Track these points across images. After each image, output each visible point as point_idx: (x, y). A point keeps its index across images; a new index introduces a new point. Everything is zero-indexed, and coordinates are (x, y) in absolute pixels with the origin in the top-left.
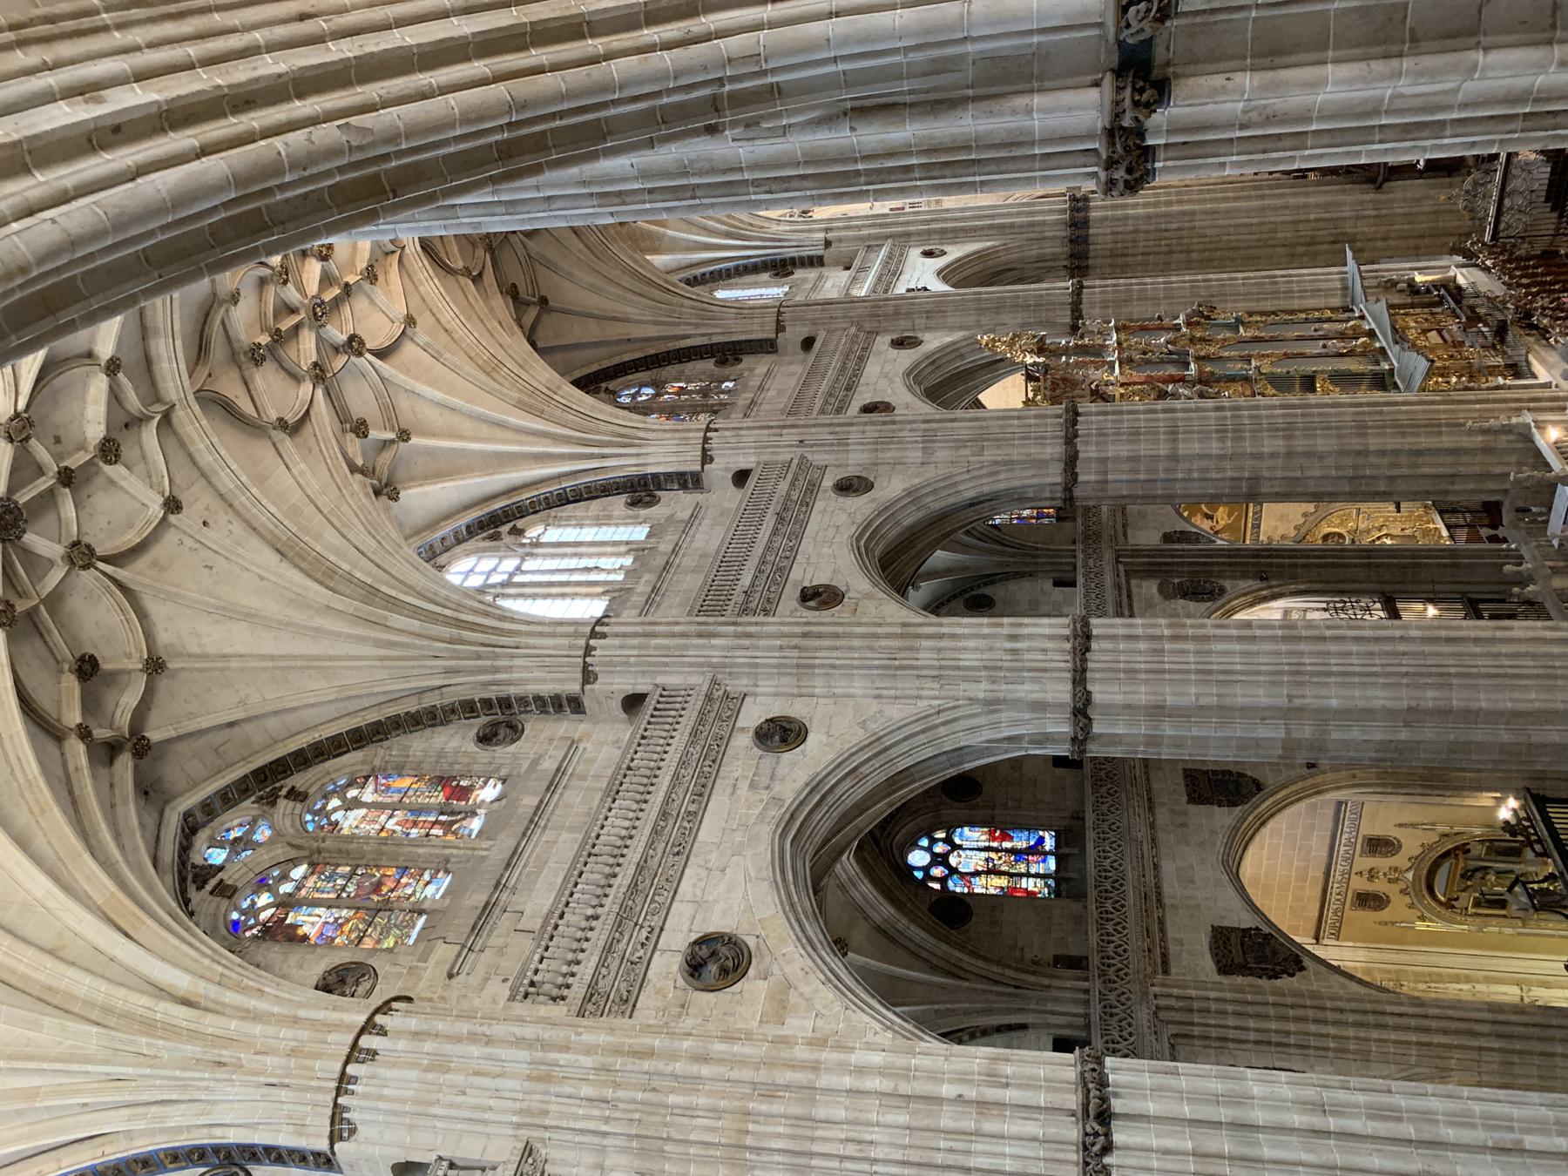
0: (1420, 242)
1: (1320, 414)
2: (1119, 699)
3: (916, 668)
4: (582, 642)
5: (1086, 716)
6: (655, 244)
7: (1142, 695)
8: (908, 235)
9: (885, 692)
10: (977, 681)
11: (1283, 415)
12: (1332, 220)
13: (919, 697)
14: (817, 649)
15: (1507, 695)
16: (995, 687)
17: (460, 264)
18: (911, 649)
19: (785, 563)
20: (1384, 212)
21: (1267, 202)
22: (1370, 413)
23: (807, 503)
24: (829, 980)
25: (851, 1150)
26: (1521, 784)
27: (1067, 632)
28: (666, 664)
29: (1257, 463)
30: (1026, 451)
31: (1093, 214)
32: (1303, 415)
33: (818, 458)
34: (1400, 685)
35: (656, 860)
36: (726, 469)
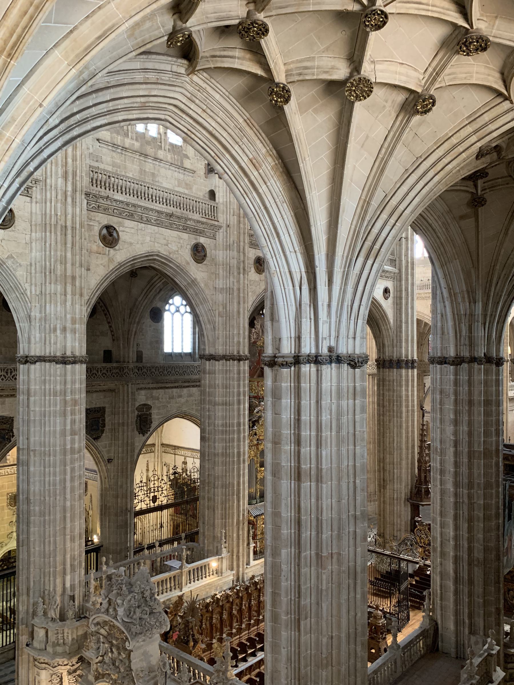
0: (382, 517)
1: (233, 469)
2: (32, 376)
3: (45, 283)
8: (400, 280)
9: (33, 268)
10: (41, 312)
11: (233, 453)
12: (394, 479)
13: (31, 285)
14: (56, 233)
16: (37, 320)
20: (395, 501)
21: (404, 451)
22: (233, 490)
23: (185, 229)
26: (104, 544)
27: (77, 354)
30: (220, 337)
31: (404, 371)
32: (234, 461)
33: (220, 235)
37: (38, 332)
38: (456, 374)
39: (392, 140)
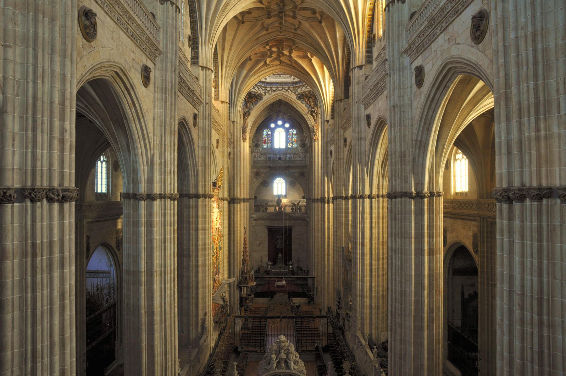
4: (175, 2)
5: (147, 199)
7: (156, 219)
8: (234, 148)
13: (154, 135)
15: (159, 343)
18: (171, 134)
19: (182, 90)
24: (83, 77)
25: (40, 70)
28: (167, 34)
33: (201, 108)
35: (117, 9)
36: (199, 75)
37: (158, 174)
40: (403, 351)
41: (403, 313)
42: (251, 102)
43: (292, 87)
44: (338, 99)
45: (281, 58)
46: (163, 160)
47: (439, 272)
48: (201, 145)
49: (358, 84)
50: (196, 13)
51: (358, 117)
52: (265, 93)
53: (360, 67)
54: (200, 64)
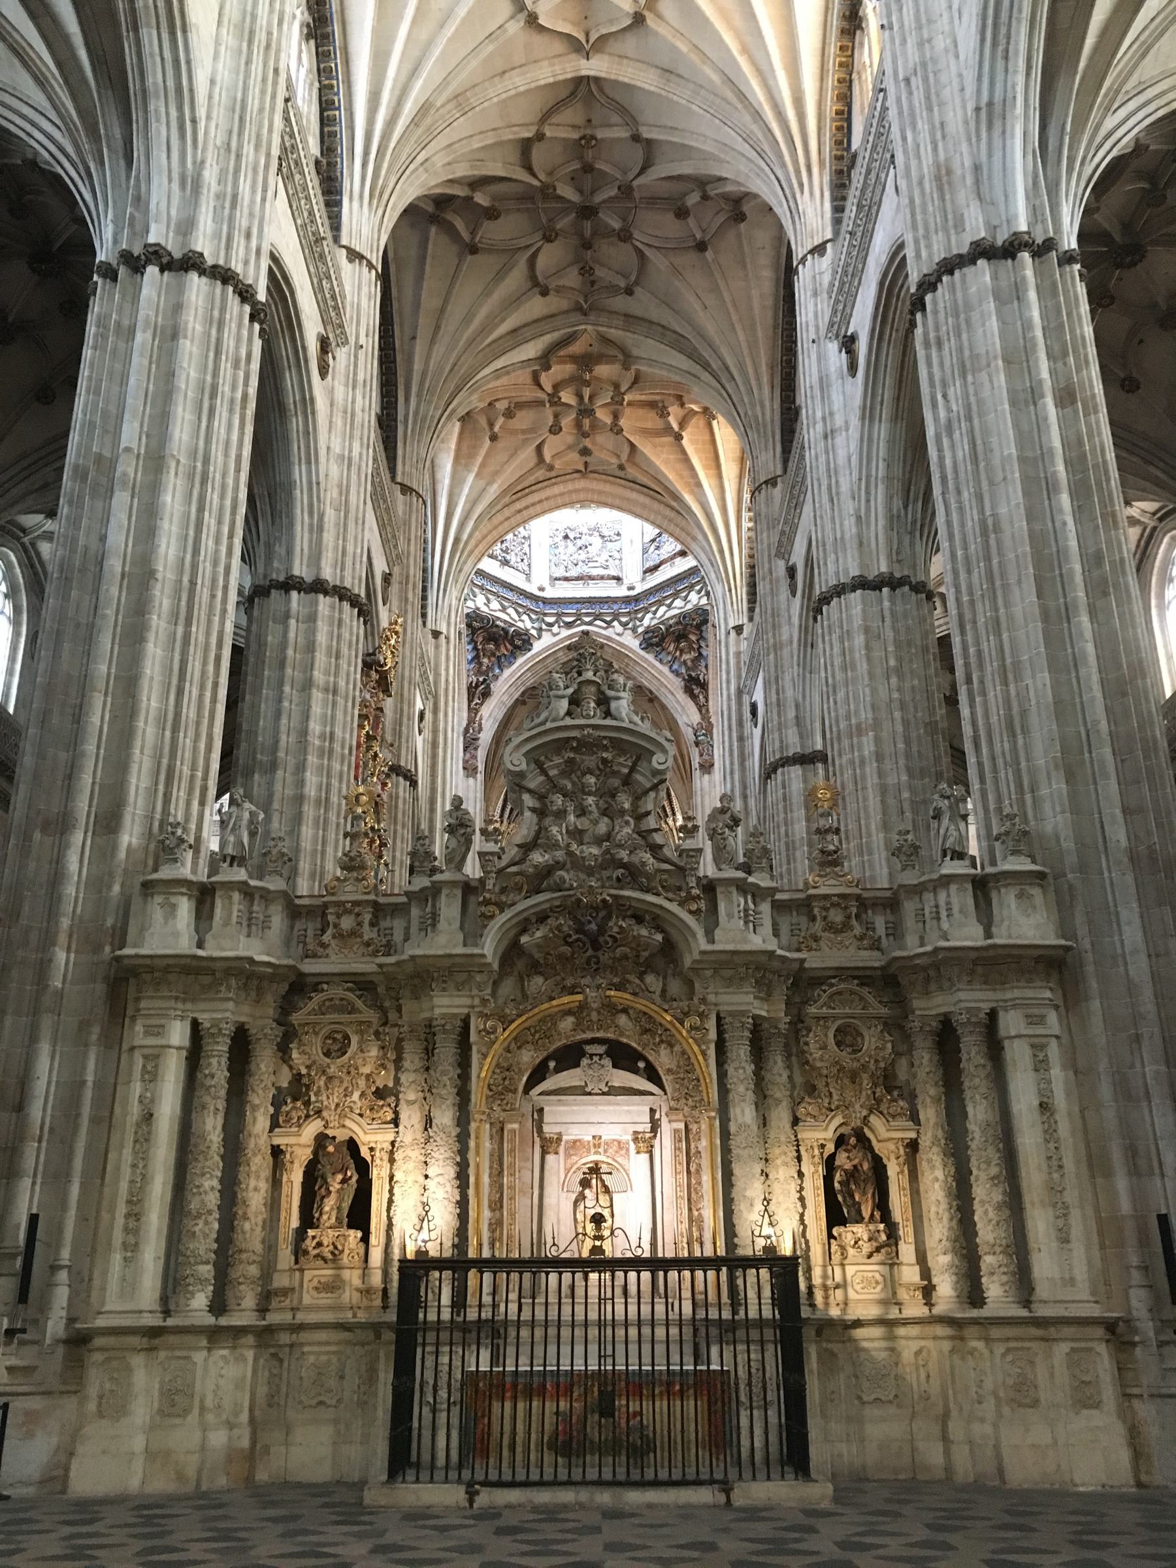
3: (240, 133)
6: (462, 458)
7: (193, 322)
17: (548, 132)
29: (290, 767)
34: (181, 572)
37: (211, 215)
38: (892, 601)
39: (1160, 24)
40: (1015, 705)
41: (998, 583)
42: (493, 655)
43: (624, 614)
44: (763, 479)
45: (587, 442)
46: (229, 189)
47: (1105, 462)
48: (337, 448)
49: (815, 294)
50: (339, 109)
51: (821, 379)
52: (540, 630)
53: (819, 250)
54: (344, 242)
